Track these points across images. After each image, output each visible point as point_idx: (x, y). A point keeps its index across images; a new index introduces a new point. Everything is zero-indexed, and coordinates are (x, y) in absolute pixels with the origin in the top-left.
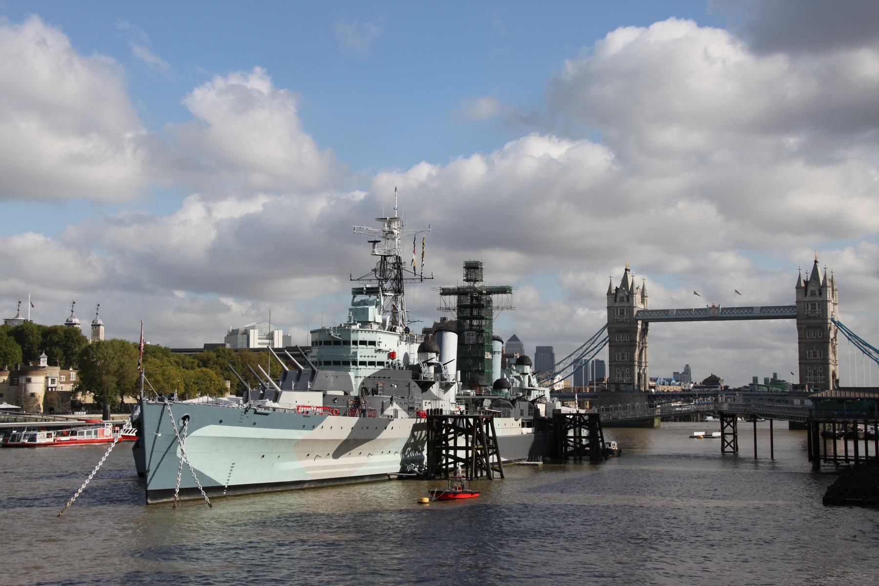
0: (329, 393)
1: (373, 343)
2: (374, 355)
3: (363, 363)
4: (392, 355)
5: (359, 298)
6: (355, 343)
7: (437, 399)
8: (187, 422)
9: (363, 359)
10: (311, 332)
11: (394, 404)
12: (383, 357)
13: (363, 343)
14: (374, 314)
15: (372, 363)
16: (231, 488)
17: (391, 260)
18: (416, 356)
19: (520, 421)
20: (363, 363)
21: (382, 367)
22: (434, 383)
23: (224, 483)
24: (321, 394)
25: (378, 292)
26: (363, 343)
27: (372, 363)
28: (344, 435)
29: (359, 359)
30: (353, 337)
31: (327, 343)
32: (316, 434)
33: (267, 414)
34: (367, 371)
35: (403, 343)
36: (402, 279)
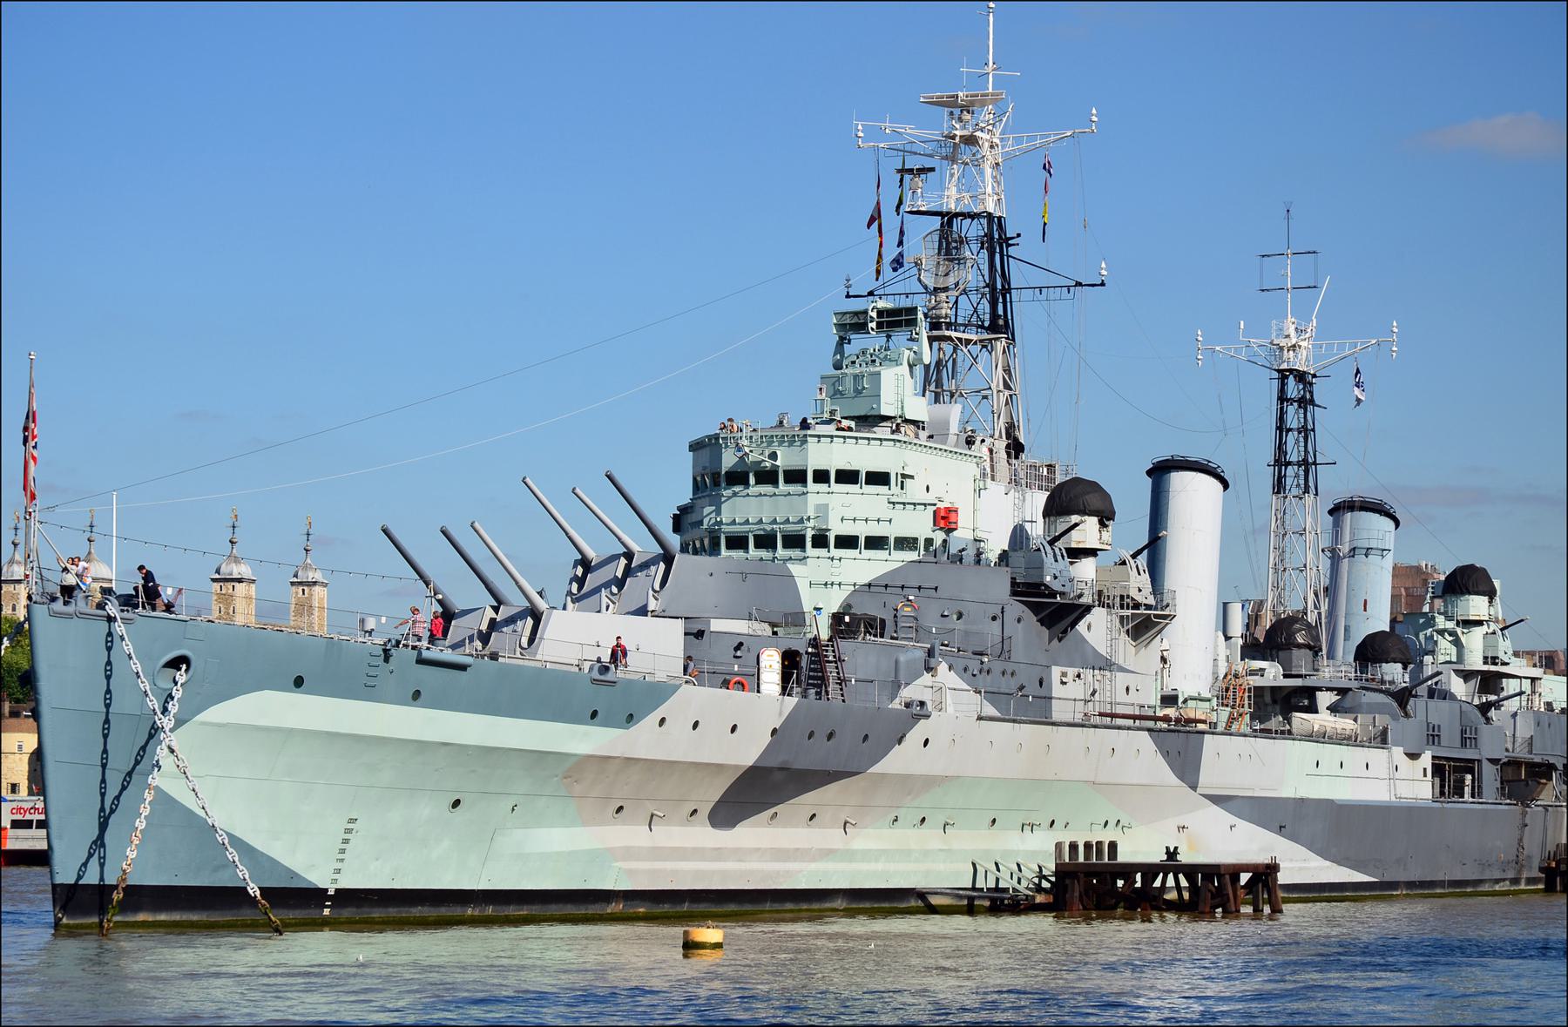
0: (717, 625)
2: (887, 512)
3: (847, 542)
5: (858, 342)
6: (821, 476)
7: (1106, 665)
8: (181, 677)
9: (847, 529)
10: (696, 447)
11: (943, 668)
12: (920, 526)
13: (847, 477)
14: (898, 389)
15: (875, 543)
16: (346, 897)
17: (973, 230)
18: (1037, 530)
19: (1426, 760)
20: (847, 542)
21: (912, 556)
22: (1088, 609)
23: (321, 877)
24: (678, 626)
25: (912, 323)
26: (847, 477)
27: (875, 543)
28: (748, 751)
29: (836, 528)
31: (737, 477)
32: (642, 740)
33: (462, 667)
34: (865, 567)
35: (996, 490)
36: (1007, 290)
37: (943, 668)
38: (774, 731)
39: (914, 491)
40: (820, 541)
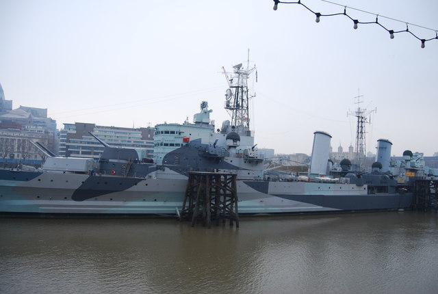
0: (110, 160)
1: (173, 132)
3: (166, 145)
4: (186, 140)
6: (162, 132)
7: (238, 168)
9: (167, 142)
13: (167, 132)
15: (172, 145)
19: (366, 186)
20: (166, 145)
26: (167, 132)
27: (172, 145)
30: (161, 129)
32: (33, 183)
34: (169, 150)
37: (167, 169)
38: (83, 182)
39: (182, 135)
40: (162, 145)
